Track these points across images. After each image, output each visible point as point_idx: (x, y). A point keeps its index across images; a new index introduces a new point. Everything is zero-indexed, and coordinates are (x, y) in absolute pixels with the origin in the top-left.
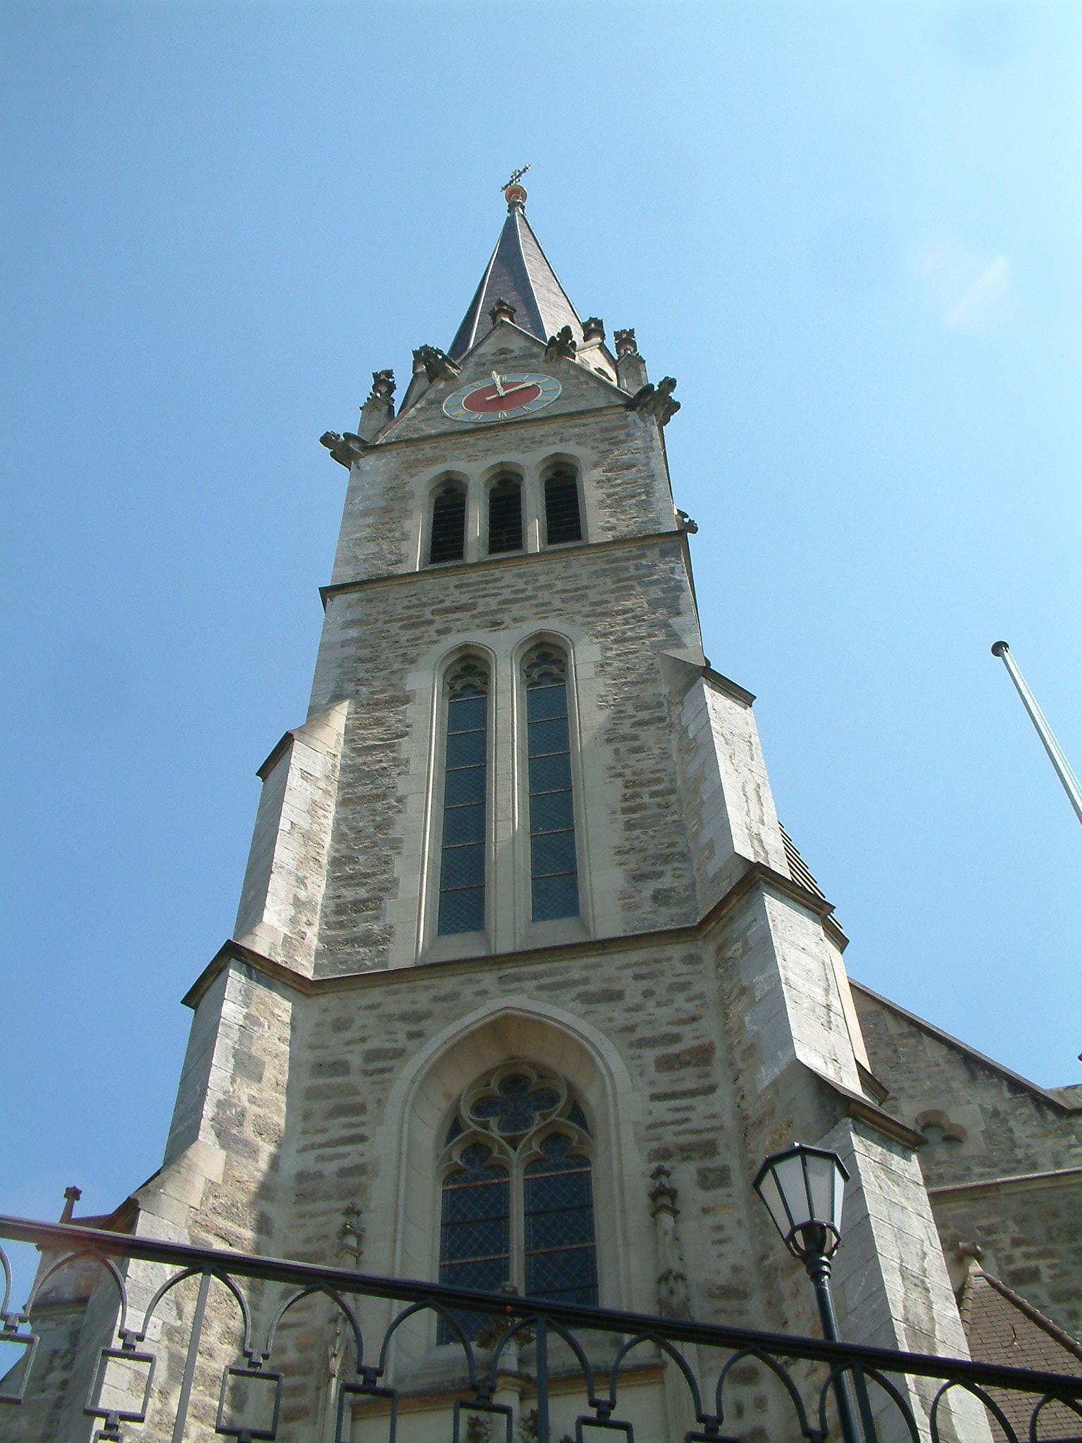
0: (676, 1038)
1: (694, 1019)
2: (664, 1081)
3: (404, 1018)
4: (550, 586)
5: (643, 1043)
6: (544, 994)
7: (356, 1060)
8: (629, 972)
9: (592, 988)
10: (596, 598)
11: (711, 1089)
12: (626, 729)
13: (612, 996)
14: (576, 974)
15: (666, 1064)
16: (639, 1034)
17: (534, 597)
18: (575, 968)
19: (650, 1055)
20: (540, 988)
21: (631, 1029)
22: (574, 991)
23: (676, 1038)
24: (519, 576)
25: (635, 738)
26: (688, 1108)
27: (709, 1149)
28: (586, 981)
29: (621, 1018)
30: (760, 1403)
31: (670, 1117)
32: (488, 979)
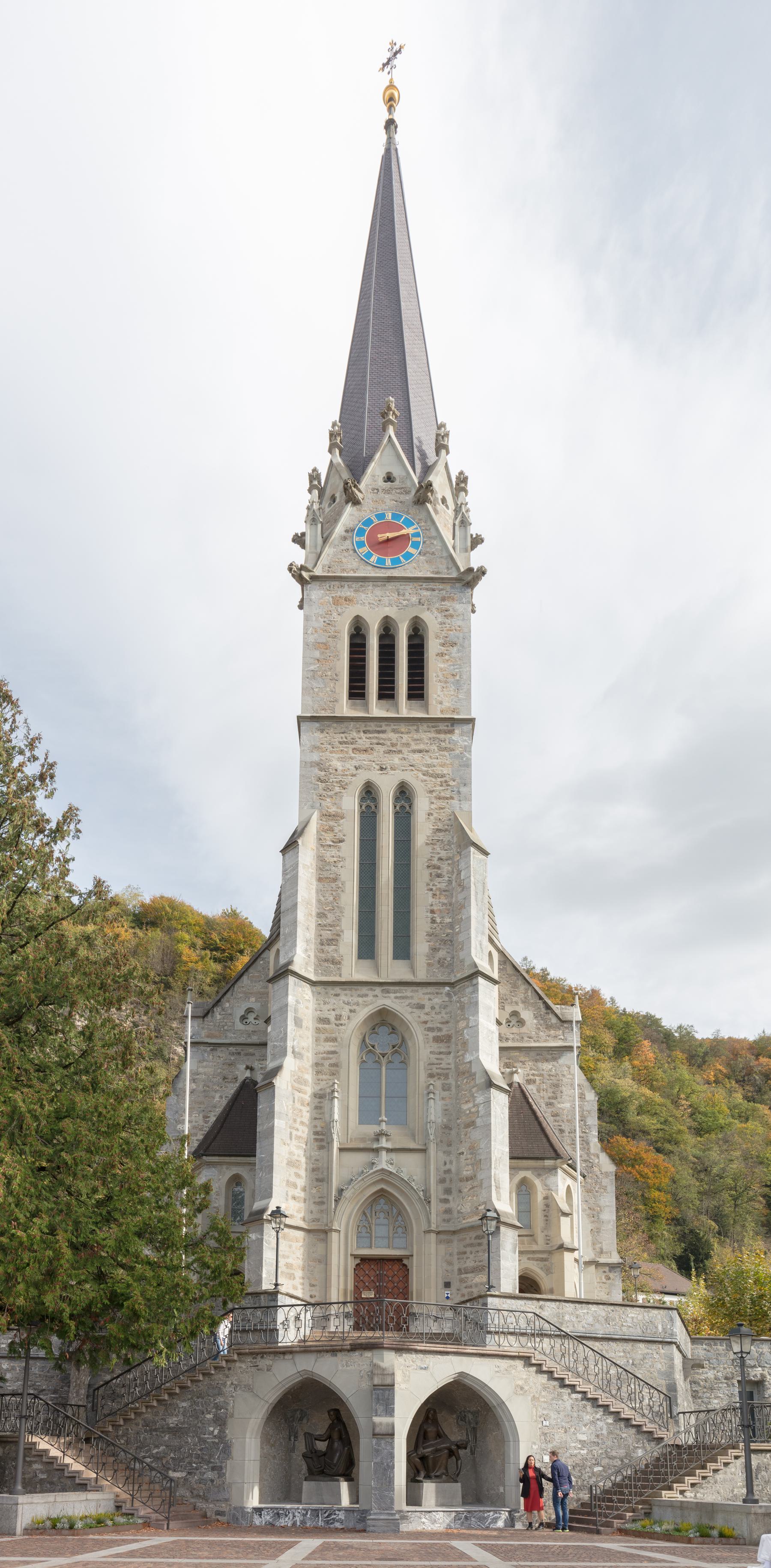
0: (440, 1030)
1: (447, 1022)
2: (435, 1047)
3: (348, 1003)
4: (407, 745)
5: (430, 1029)
6: (397, 1001)
7: (332, 1019)
8: (427, 997)
9: (415, 1001)
10: (429, 761)
11: (450, 1053)
12: (435, 862)
13: (421, 1007)
14: (409, 994)
15: (437, 1039)
16: (429, 1025)
17: (400, 752)
18: (408, 991)
19: (431, 1035)
20: (396, 998)
21: (426, 1022)
22: (408, 1001)
23: (440, 1030)
24: (394, 731)
25: (439, 868)
26: (441, 1059)
27: (446, 1076)
28: (412, 997)
29: (425, 1018)
30: (451, 1162)
31: (436, 1061)
32: (378, 990)
